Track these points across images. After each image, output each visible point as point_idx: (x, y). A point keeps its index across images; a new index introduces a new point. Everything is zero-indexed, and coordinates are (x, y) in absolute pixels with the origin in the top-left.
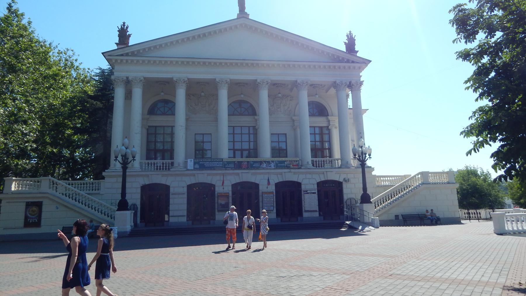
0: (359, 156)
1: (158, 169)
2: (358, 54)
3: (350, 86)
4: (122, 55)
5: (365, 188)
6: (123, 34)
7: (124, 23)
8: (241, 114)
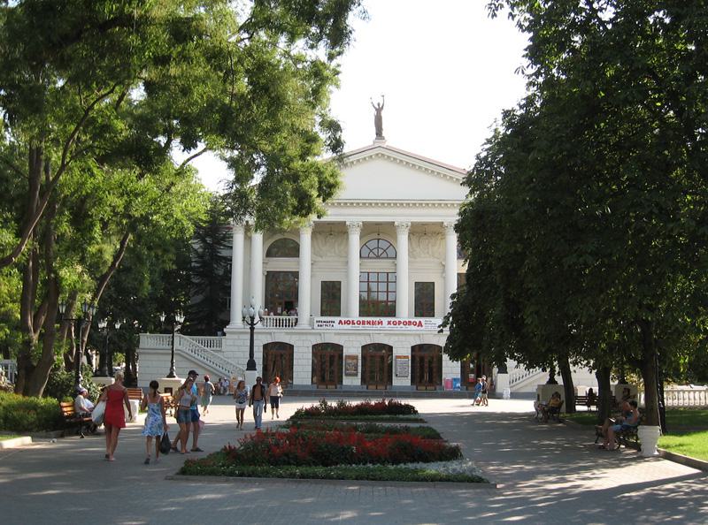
8: (378, 257)
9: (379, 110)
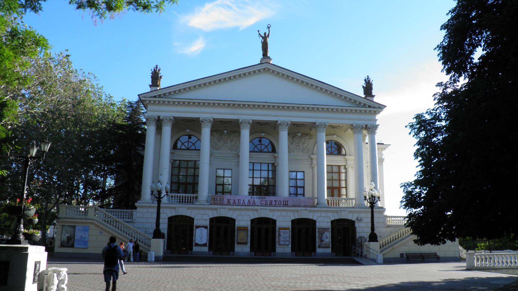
1: (181, 201)
2: (375, 100)
3: (366, 128)
4: (155, 97)
6: (156, 77)
7: (157, 66)
8: (261, 151)
9: (265, 38)
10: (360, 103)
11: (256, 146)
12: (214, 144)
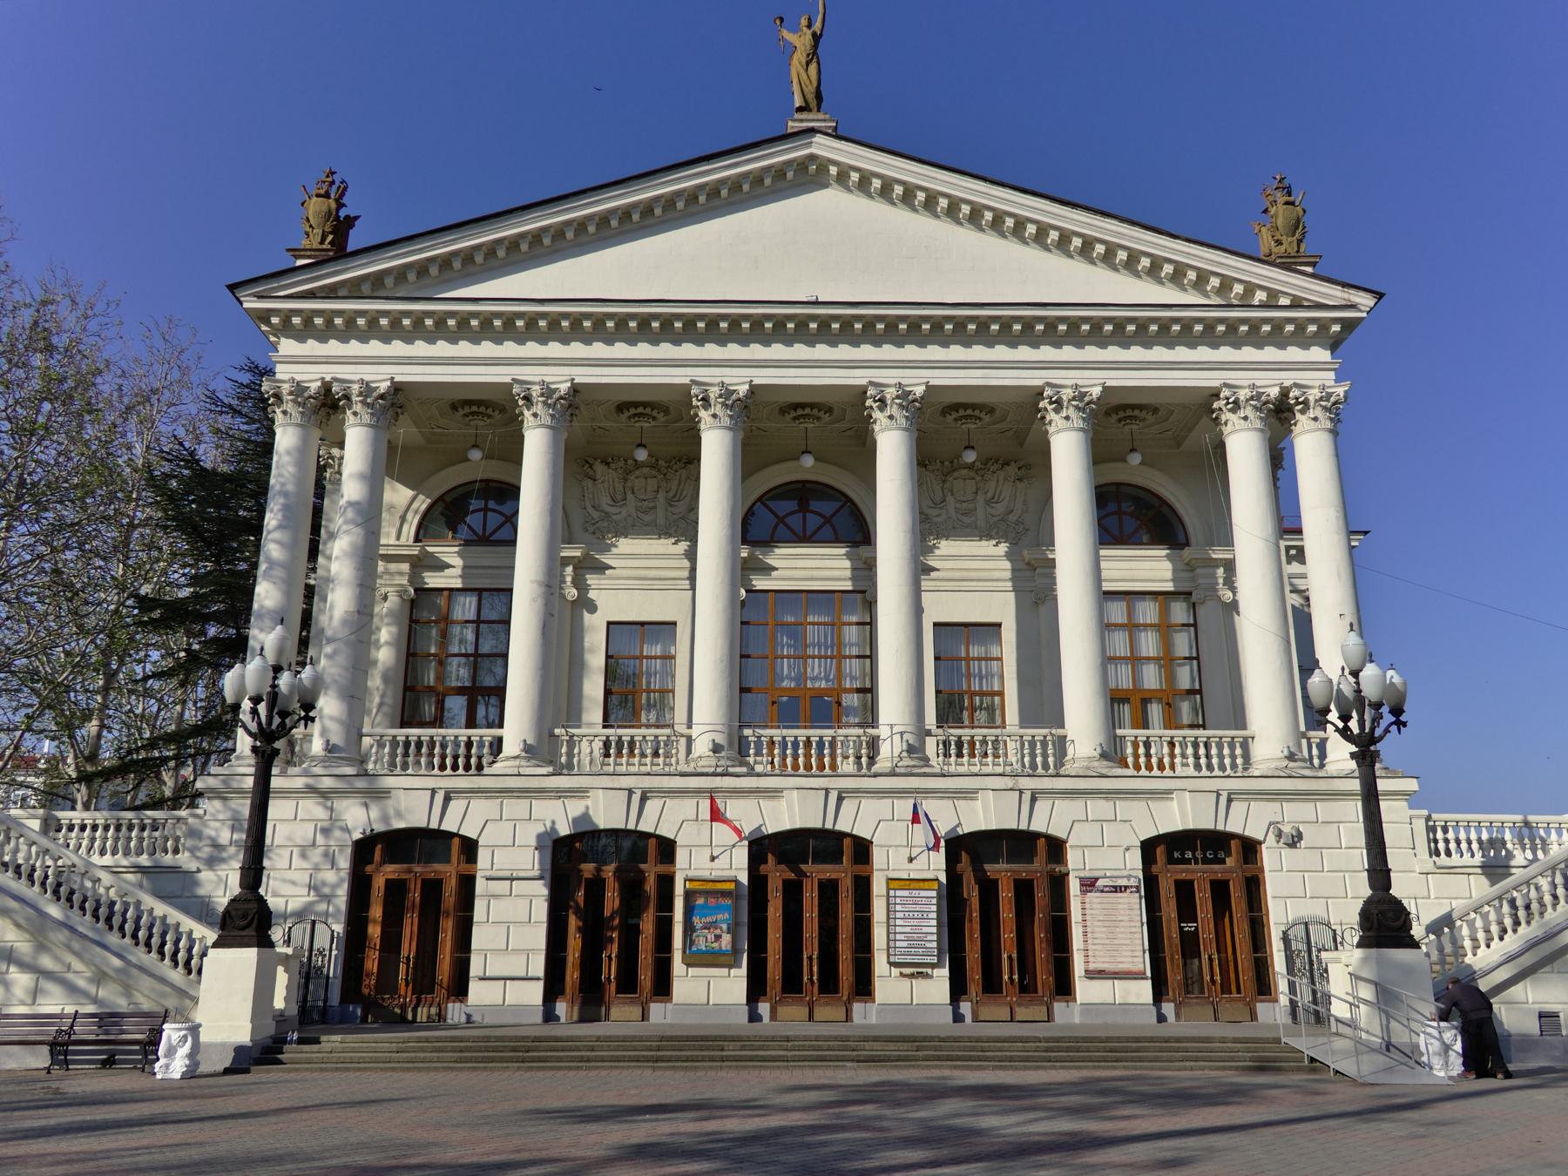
0: (1345, 718)
5: (1379, 873)
10: (1250, 289)
11: (781, 520)
12: (595, 514)
